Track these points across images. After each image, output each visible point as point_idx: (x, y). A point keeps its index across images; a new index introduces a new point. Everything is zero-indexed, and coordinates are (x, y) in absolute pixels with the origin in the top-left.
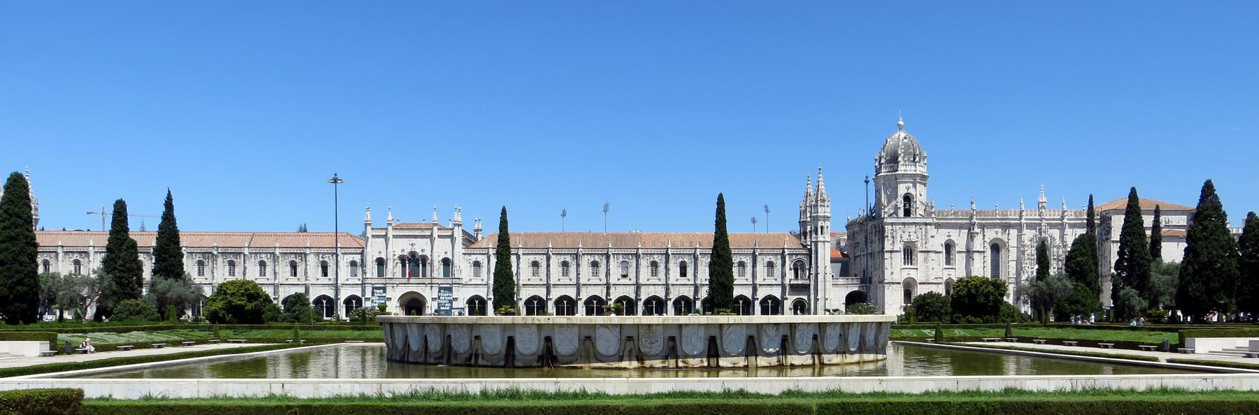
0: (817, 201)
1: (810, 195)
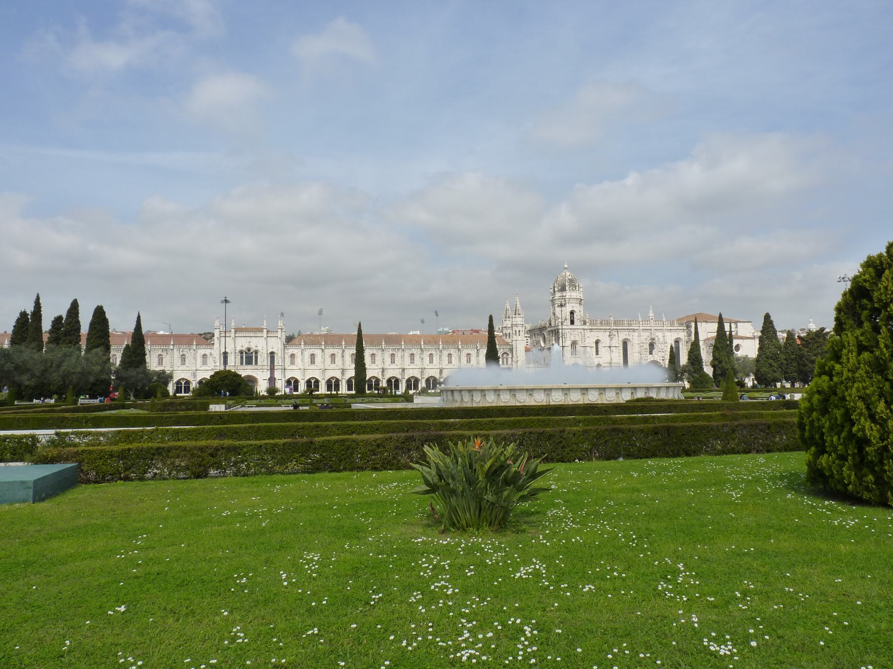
0: (515, 314)
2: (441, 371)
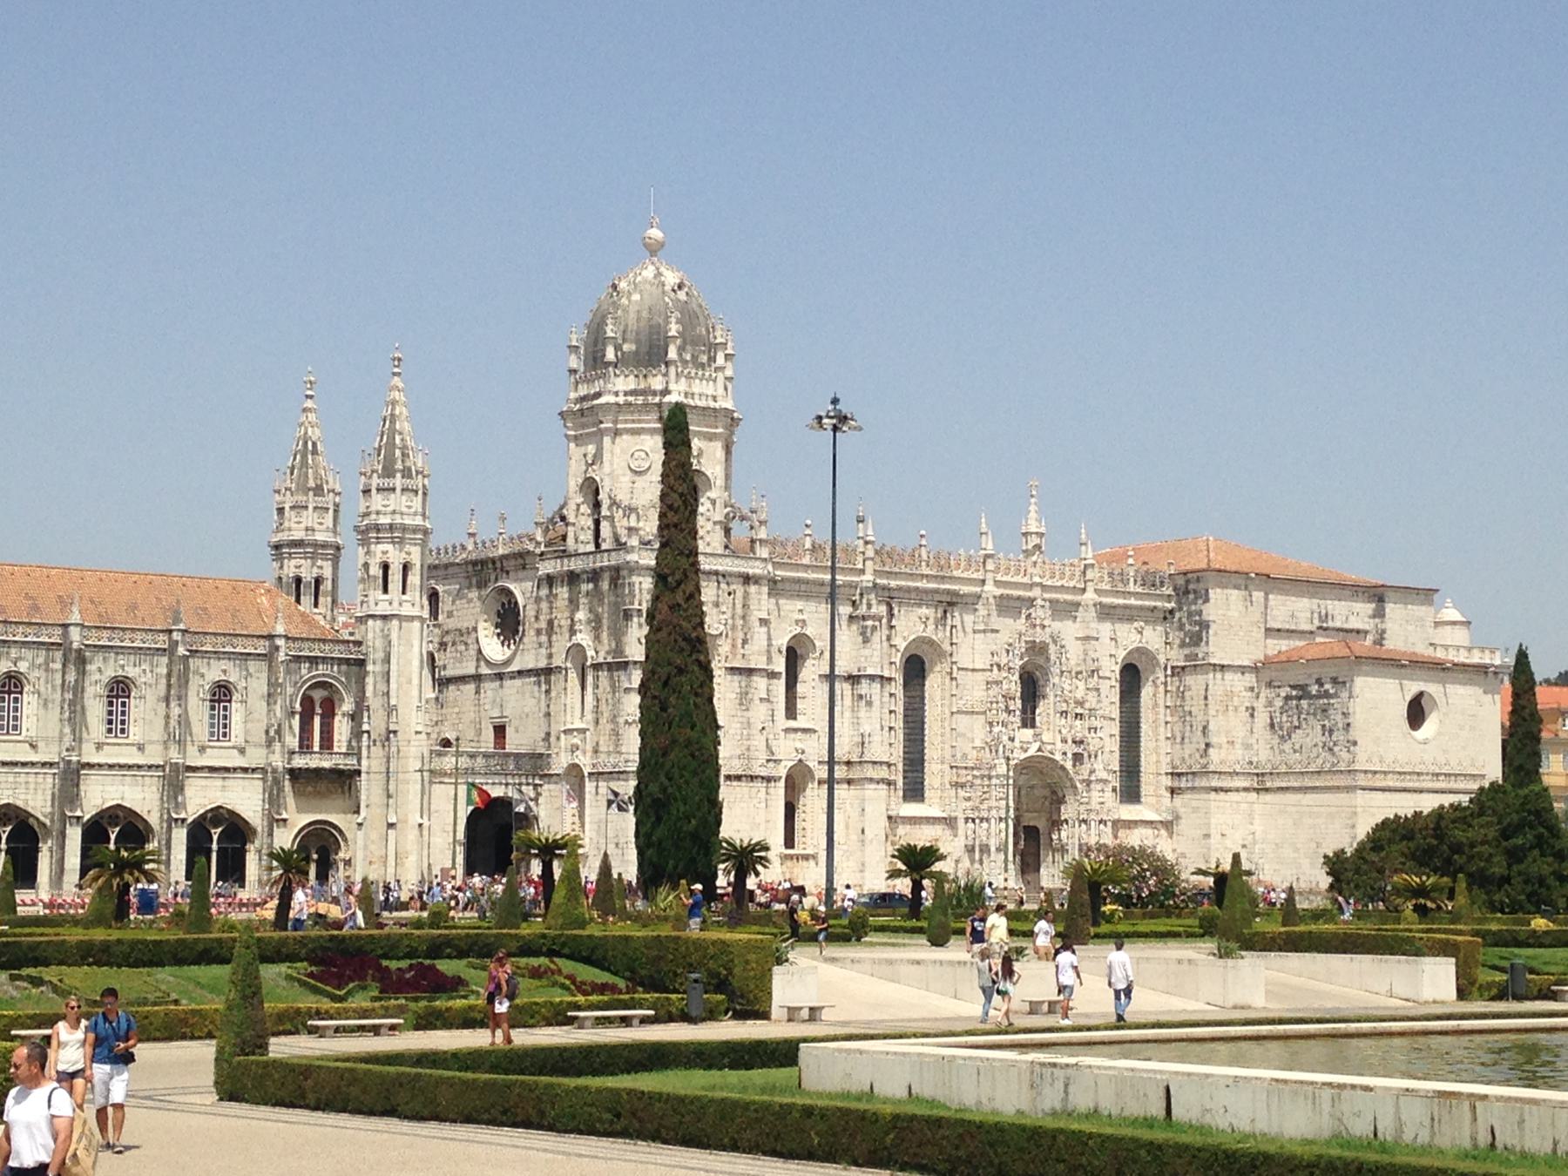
1: (315, 452)
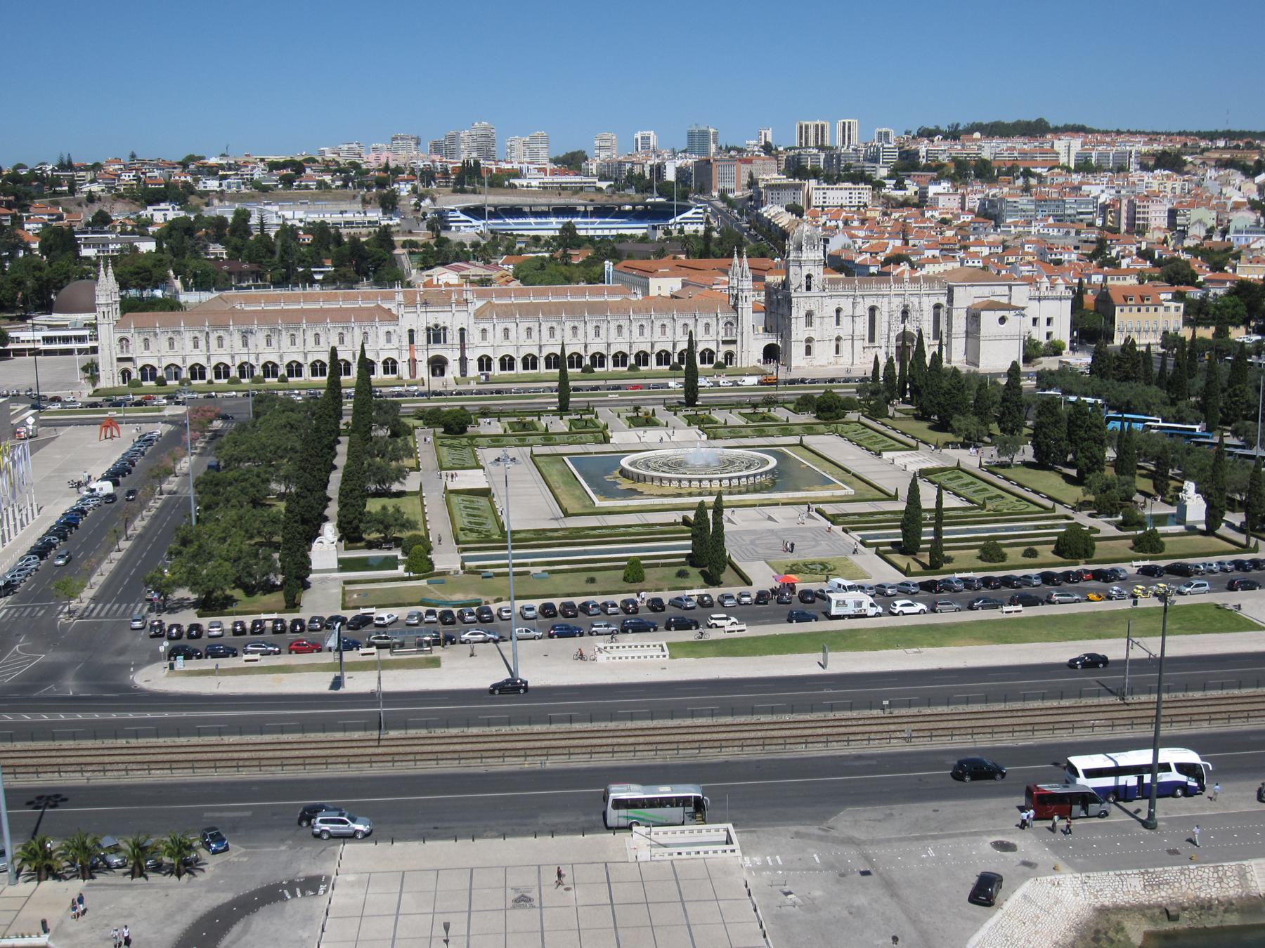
2: (652, 346)
